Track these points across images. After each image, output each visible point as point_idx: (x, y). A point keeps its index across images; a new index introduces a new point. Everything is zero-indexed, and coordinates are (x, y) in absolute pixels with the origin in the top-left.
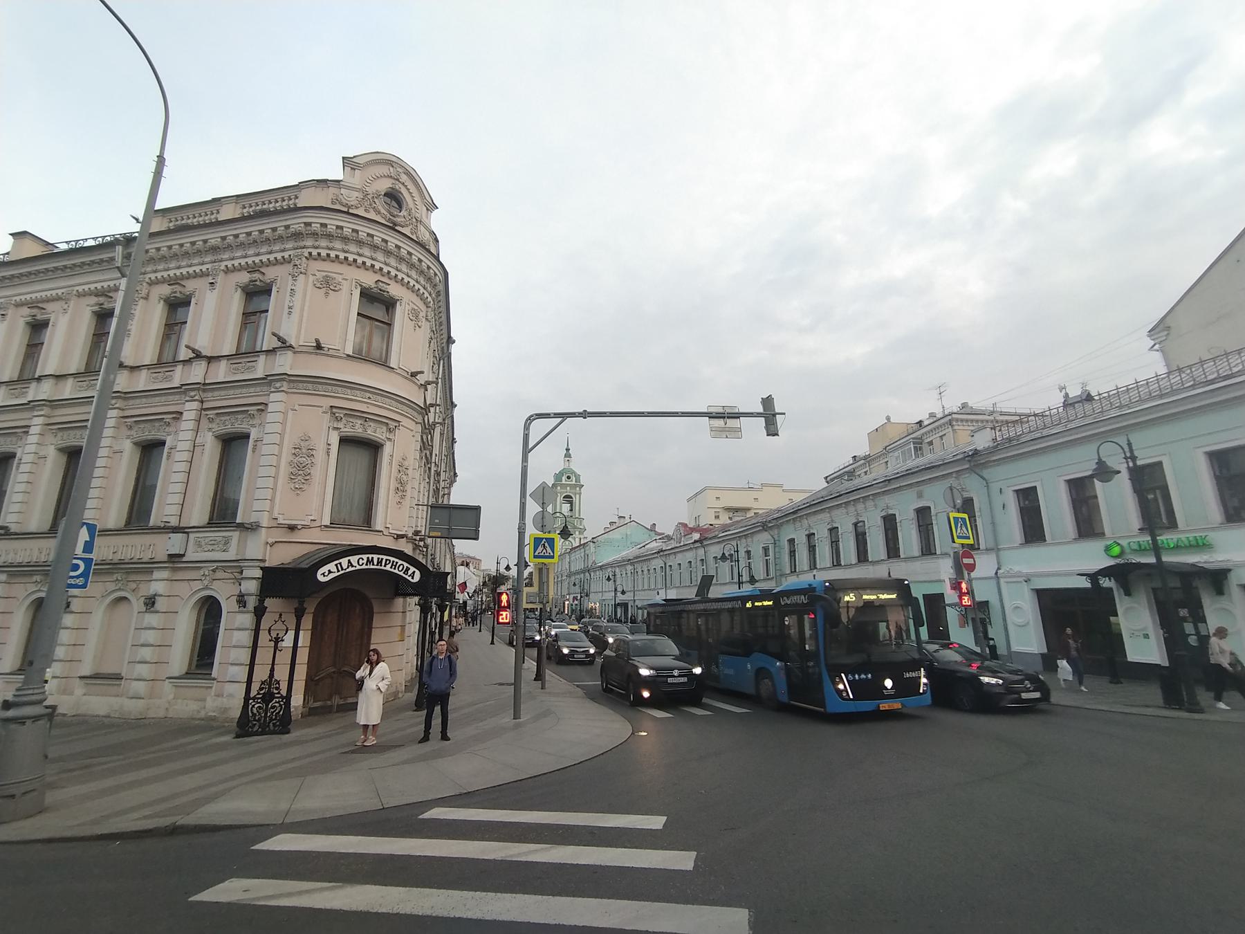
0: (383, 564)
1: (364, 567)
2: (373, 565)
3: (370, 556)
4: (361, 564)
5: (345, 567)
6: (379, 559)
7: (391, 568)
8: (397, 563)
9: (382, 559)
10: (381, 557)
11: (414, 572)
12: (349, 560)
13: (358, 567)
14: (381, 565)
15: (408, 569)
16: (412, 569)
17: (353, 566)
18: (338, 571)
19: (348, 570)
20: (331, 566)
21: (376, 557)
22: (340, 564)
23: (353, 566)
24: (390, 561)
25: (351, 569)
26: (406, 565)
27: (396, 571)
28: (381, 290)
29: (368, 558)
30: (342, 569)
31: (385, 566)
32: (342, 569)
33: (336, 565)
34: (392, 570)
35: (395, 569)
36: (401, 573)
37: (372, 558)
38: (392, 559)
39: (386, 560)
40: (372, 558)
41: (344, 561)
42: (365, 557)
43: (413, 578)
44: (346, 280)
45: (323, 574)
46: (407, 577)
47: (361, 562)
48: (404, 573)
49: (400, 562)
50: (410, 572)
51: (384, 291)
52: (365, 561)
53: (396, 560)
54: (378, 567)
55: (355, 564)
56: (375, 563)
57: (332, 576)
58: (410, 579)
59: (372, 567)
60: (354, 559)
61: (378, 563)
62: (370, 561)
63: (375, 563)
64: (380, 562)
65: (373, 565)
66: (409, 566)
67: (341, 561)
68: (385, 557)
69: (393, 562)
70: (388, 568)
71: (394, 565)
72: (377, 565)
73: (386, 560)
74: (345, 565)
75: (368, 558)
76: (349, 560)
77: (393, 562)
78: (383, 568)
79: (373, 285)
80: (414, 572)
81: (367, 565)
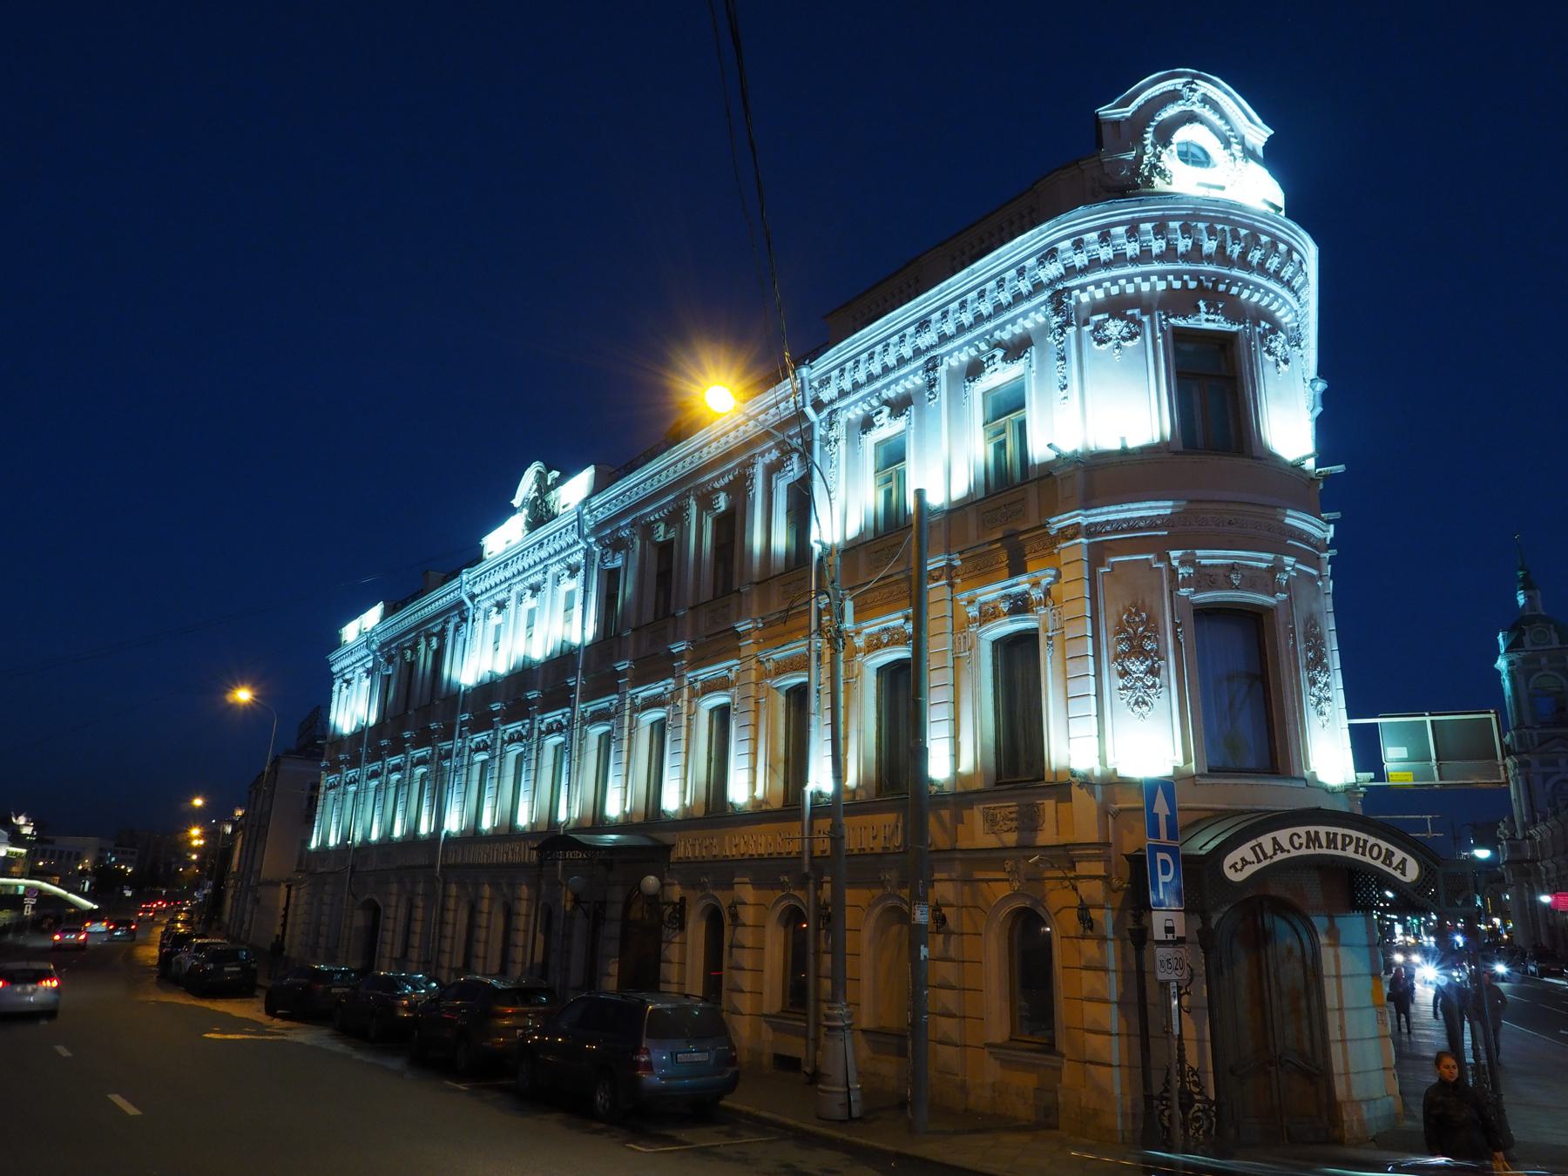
0: (1339, 846)
1: (1304, 851)
2: (1321, 846)
3: (1312, 829)
4: (1297, 845)
5: (1269, 852)
6: (1328, 834)
8: (1365, 842)
10: (1332, 830)
11: (1404, 861)
12: (1274, 839)
13: (1294, 853)
15: (1390, 854)
16: (1399, 855)
17: (1283, 850)
18: (1259, 861)
19: (1276, 859)
20: (1245, 851)
21: (1322, 830)
22: (1260, 845)
23: (1283, 850)
24: (1350, 837)
25: (1280, 856)
26: (1384, 845)
27: (1367, 859)
29: (1308, 833)
30: (1266, 857)
31: (1343, 849)
33: (1253, 848)
34: (1359, 857)
35: (1363, 854)
36: (1378, 864)
38: (1355, 834)
39: (1344, 836)
40: (1317, 833)
41: (1266, 840)
42: (1302, 830)
43: (1403, 873)
45: (1233, 866)
46: (1390, 870)
47: (1297, 841)
48: (1384, 862)
49: (1372, 840)
50: (1396, 860)
52: (1303, 840)
53: (1363, 836)
54: (1332, 852)
55: (1287, 846)
56: (1324, 843)
57: (1249, 870)
58: (1397, 874)
59: (1318, 851)
60: (1283, 835)
62: (1313, 840)
63: (1324, 843)
64: (1332, 841)
65: (1321, 846)
66: (1392, 848)
67: (1261, 839)
68: (1340, 831)
70: (1350, 852)
71: (1361, 847)
73: (1344, 836)
74: (1269, 852)
75: (1308, 833)
76: (1274, 839)
78: (1339, 853)
80: (1404, 861)
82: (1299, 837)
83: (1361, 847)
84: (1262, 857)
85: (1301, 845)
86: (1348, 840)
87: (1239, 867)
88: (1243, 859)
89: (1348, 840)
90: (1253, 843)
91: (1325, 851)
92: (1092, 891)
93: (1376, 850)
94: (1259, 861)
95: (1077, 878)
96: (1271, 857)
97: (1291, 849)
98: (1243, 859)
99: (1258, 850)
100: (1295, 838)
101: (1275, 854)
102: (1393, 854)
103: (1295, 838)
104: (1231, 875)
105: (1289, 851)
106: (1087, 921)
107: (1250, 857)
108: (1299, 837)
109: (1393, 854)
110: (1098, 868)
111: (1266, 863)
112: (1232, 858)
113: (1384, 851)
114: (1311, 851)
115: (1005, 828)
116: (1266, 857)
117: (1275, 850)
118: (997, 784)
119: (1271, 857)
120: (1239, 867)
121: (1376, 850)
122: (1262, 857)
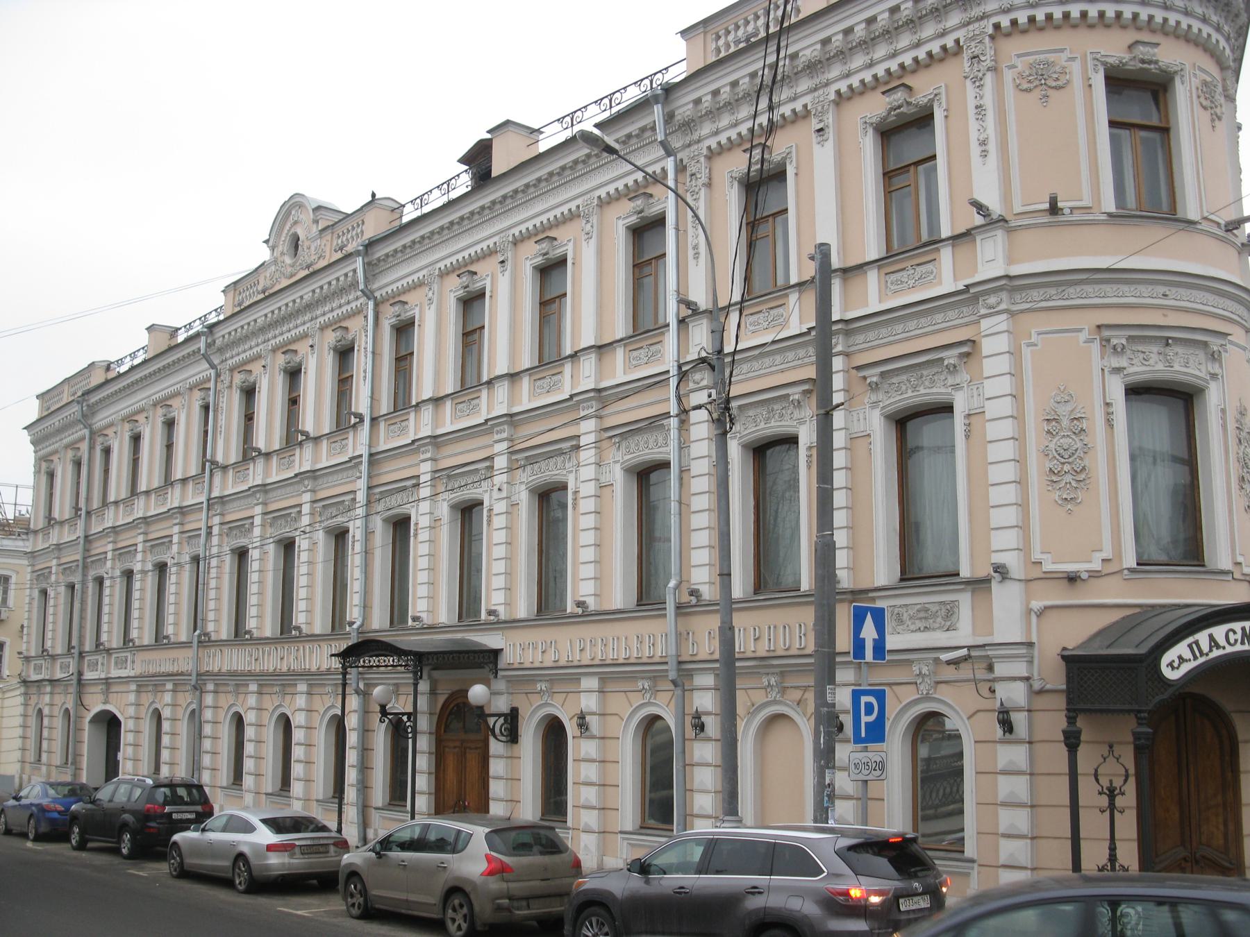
1: (1239, 648)
4: (1232, 641)
5: (1205, 648)
12: (1211, 636)
13: (1229, 649)
17: (1218, 647)
18: (1195, 658)
19: (1212, 655)
20: (1182, 649)
22: (1197, 643)
23: (1218, 647)
25: (1216, 653)
28: (1143, 61)
29: (1243, 629)
33: (1190, 646)
41: (1202, 637)
42: (1237, 626)
44: (1072, 59)
45: (1171, 665)
47: (1232, 637)
51: (1150, 62)
52: (1239, 636)
55: (1222, 642)
57: (1186, 668)
60: (1219, 632)
74: (1205, 648)
76: (1211, 636)
79: (1126, 57)
81: (1242, 643)
82: (1235, 633)
84: (1198, 654)
85: (1236, 641)
87: (1176, 665)
88: (1180, 657)
90: (1190, 640)
92: (1015, 694)
94: (1195, 658)
95: (994, 680)
96: (1207, 655)
97: (1227, 646)
98: (1180, 657)
99: (1195, 648)
100: (1231, 634)
101: (1211, 650)
103: (1231, 634)
104: (1171, 675)
105: (1224, 648)
106: (1007, 725)
107: (1187, 654)
108: (1235, 633)
110: (1020, 669)
111: (1201, 660)
112: (1170, 656)
115: (912, 627)
116: (1202, 654)
117: (1211, 648)
118: (902, 580)
119: (1207, 655)
120: (1176, 665)
122: (1198, 654)
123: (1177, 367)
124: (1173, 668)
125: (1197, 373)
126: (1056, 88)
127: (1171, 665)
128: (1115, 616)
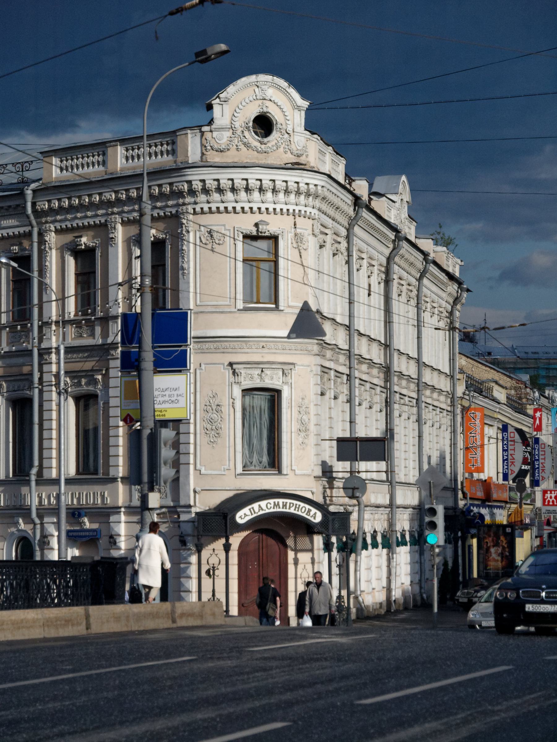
1: (272, 510)
3: (276, 500)
4: (269, 507)
5: (256, 509)
6: (283, 502)
7: (295, 510)
8: (299, 505)
9: (286, 503)
10: (285, 500)
11: (315, 514)
12: (260, 506)
13: (267, 511)
14: (286, 508)
15: (309, 511)
16: (314, 510)
18: (252, 514)
21: (281, 501)
22: (253, 508)
23: (262, 510)
24: (293, 504)
25: (261, 512)
26: (308, 507)
27: (299, 513)
29: (274, 502)
31: (289, 509)
32: (255, 513)
33: (250, 509)
34: (296, 512)
35: (298, 511)
36: (304, 515)
37: (278, 502)
38: (295, 502)
39: (290, 503)
40: (278, 502)
41: (255, 506)
42: (272, 501)
43: (315, 518)
45: (241, 517)
47: (269, 506)
48: (307, 514)
49: (302, 504)
50: (312, 513)
52: (272, 505)
53: (298, 503)
54: (284, 510)
55: (264, 507)
56: (281, 506)
58: (312, 519)
59: (278, 510)
60: (263, 503)
61: (286, 505)
62: (276, 505)
63: (281, 506)
64: (284, 506)
65: (279, 508)
68: (289, 501)
69: (296, 504)
70: (292, 510)
71: (297, 508)
72: (283, 508)
73: (290, 503)
74: (256, 509)
75: (274, 502)
76: (260, 506)
77: (296, 504)
78: (287, 510)
80: (315, 514)
81: (274, 508)
83: (297, 508)
86: (292, 505)
88: (245, 514)
89: (292, 505)
90: (250, 507)
91: (281, 510)
93: (304, 509)
98: (245, 514)
100: (269, 505)
102: (311, 510)
103: (269, 505)
107: (248, 513)
109: (311, 510)
111: (254, 515)
113: (307, 510)
114: (275, 510)
117: (259, 511)
120: (243, 517)
121: (304, 509)
123: (267, 381)
124: (242, 519)
125: (277, 383)
126: (219, 244)
127: (241, 517)
128: (231, 494)
